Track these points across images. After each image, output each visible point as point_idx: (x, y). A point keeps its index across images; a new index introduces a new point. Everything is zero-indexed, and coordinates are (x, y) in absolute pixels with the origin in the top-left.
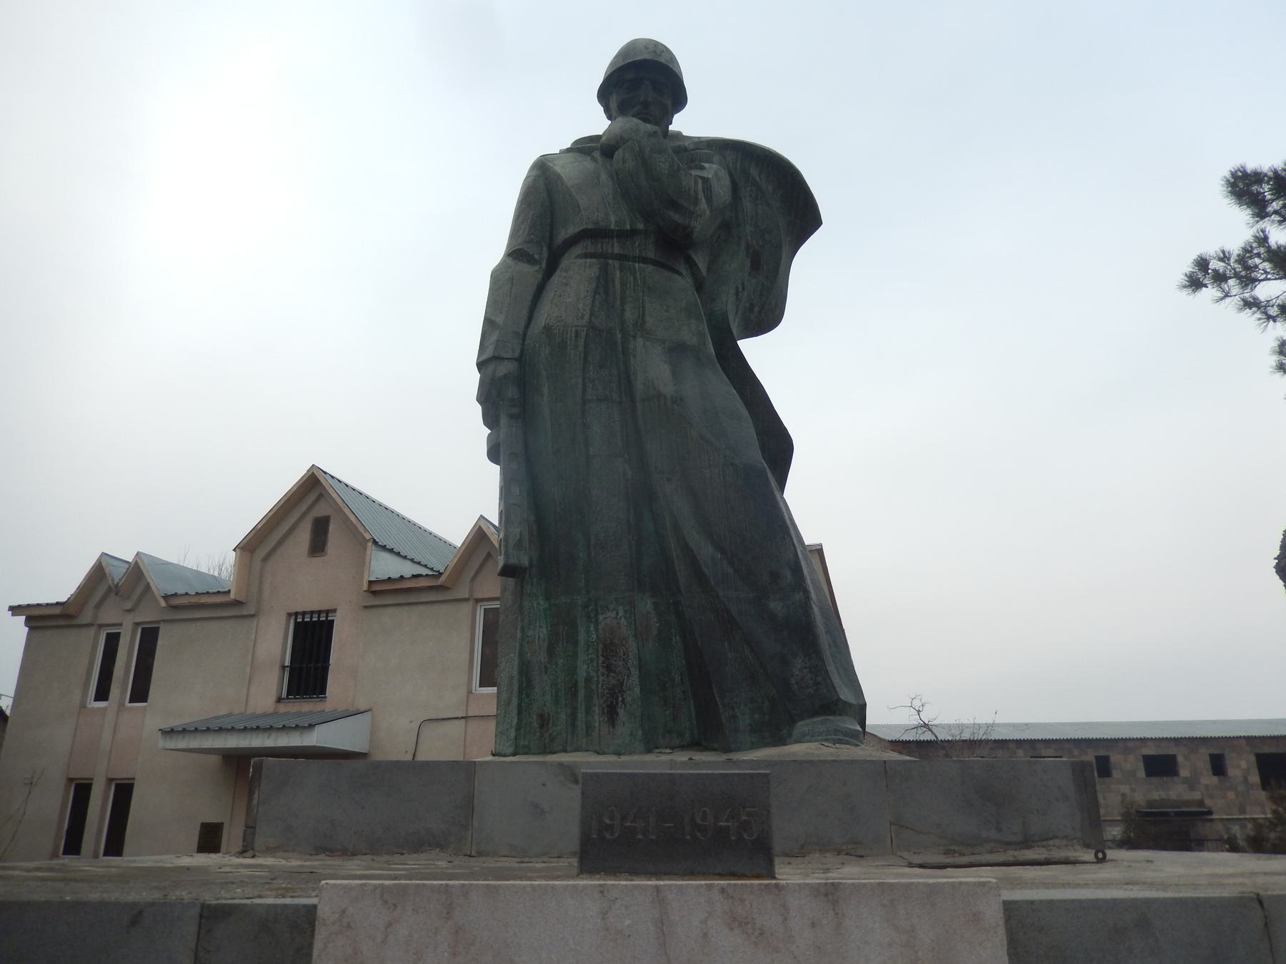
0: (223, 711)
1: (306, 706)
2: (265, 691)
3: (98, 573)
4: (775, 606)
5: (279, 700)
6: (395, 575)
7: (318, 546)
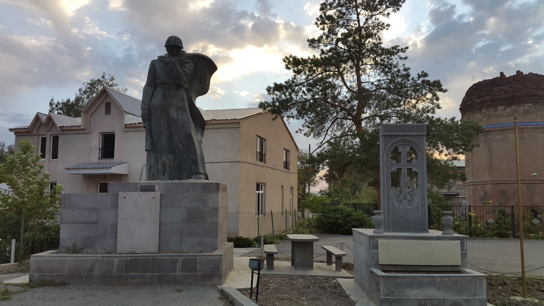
0: (82, 162)
1: (108, 161)
2: (95, 155)
3: (37, 118)
4: (191, 157)
5: (99, 159)
6: (133, 123)
7: (108, 111)
